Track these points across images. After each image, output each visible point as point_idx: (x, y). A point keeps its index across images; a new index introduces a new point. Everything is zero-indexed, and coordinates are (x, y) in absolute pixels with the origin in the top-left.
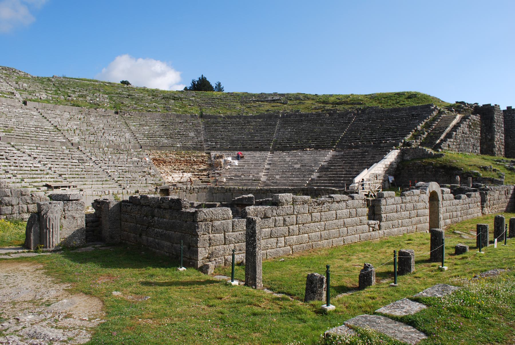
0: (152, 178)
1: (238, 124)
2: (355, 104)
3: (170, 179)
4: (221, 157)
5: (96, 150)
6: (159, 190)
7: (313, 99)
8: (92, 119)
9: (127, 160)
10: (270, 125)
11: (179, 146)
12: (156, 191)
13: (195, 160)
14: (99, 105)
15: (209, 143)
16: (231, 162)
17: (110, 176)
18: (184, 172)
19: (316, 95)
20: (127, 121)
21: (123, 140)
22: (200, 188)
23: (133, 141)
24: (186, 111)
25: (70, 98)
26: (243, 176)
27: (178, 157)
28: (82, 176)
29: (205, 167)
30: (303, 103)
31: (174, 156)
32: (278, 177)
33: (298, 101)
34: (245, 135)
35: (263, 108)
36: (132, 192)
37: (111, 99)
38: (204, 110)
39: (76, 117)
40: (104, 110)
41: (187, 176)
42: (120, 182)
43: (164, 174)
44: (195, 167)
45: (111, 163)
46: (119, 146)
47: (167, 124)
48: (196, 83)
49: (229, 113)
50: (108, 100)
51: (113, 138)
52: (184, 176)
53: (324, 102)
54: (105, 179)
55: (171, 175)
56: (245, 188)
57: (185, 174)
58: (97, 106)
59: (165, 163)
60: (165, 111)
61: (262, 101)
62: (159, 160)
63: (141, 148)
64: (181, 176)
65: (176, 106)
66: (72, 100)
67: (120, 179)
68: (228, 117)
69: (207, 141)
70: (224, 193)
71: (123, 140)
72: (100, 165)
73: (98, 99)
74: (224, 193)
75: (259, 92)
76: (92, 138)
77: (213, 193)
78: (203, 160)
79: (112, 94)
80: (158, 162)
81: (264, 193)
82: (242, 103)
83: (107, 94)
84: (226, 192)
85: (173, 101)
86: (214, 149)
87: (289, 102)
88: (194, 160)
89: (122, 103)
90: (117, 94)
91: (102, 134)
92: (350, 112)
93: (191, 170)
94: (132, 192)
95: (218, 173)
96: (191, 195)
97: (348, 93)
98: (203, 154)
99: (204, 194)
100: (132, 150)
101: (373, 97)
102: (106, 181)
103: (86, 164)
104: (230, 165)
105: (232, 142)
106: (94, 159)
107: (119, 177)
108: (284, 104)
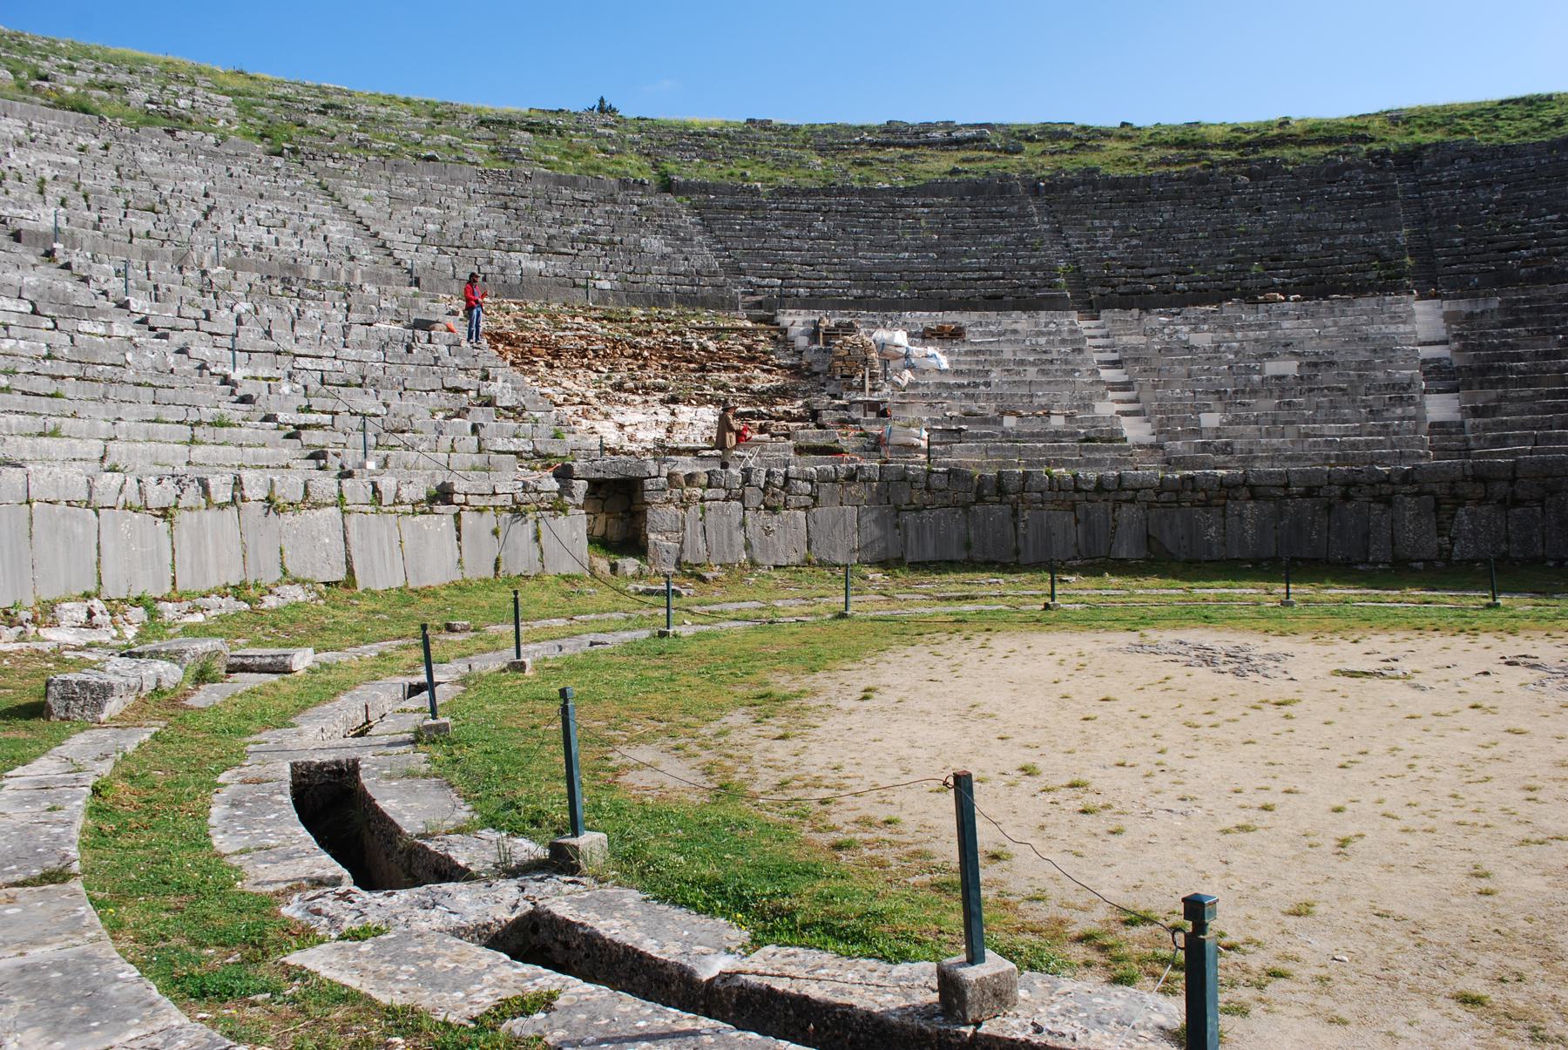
0: (512, 423)
2: (1339, 141)
4: (850, 328)
5: (164, 273)
6: (580, 487)
7: (1123, 138)
8: (145, 158)
9: (346, 331)
10: (1002, 215)
11: (606, 285)
12: (566, 490)
13: (712, 346)
14: (190, 121)
16: (907, 356)
17: (245, 399)
18: (674, 400)
19: (1123, 124)
20: (329, 181)
21: (314, 247)
22: (824, 478)
23: (365, 253)
24: (598, 169)
25: (46, 84)
26: (1010, 422)
27: (620, 332)
29: (777, 380)
30: (1098, 148)
31: (596, 326)
32: (1210, 420)
33: (1067, 145)
35: (925, 167)
36: (407, 493)
37: (246, 110)
38: (671, 167)
39: (62, 139)
40: (211, 138)
41: (698, 421)
42: (315, 438)
43: (568, 410)
44: (724, 377)
46: (294, 266)
47: (522, 203)
49: (784, 179)
50: (232, 112)
52: (682, 418)
53: (1181, 144)
54: (207, 414)
55: (607, 416)
56: (1092, 475)
57: (685, 413)
58: (175, 123)
59: (557, 355)
60: (502, 164)
61: (908, 146)
62: (524, 339)
63: (417, 283)
65: (546, 150)
66: (59, 92)
67: (312, 418)
68: (789, 192)
69: (741, 272)
70: (966, 507)
71: (314, 247)
72: (177, 339)
73: (182, 103)
74: (966, 507)
76: (142, 223)
77: (898, 510)
78: (749, 348)
81: (1206, 504)
82: (821, 151)
83: (226, 94)
84: (980, 499)
85: (527, 135)
86: (786, 300)
87: (1027, 146)
88: (705, 349)
89: (302, 125)
90: (271, 97)
91: (198, 216)
92: (1347, 166)
94: (407, 493)
95: (872, 406)
96: (773, 522)
97: (1275, 115)
98: (740, 324)
99: (851, 511)
100: (371, 289)
101: (1395, 119)
102: (219, 423)
104: (911, 367)
105: (862, 276)
106: (139, 303)
107: (309, 409)
108: (1007, 151)
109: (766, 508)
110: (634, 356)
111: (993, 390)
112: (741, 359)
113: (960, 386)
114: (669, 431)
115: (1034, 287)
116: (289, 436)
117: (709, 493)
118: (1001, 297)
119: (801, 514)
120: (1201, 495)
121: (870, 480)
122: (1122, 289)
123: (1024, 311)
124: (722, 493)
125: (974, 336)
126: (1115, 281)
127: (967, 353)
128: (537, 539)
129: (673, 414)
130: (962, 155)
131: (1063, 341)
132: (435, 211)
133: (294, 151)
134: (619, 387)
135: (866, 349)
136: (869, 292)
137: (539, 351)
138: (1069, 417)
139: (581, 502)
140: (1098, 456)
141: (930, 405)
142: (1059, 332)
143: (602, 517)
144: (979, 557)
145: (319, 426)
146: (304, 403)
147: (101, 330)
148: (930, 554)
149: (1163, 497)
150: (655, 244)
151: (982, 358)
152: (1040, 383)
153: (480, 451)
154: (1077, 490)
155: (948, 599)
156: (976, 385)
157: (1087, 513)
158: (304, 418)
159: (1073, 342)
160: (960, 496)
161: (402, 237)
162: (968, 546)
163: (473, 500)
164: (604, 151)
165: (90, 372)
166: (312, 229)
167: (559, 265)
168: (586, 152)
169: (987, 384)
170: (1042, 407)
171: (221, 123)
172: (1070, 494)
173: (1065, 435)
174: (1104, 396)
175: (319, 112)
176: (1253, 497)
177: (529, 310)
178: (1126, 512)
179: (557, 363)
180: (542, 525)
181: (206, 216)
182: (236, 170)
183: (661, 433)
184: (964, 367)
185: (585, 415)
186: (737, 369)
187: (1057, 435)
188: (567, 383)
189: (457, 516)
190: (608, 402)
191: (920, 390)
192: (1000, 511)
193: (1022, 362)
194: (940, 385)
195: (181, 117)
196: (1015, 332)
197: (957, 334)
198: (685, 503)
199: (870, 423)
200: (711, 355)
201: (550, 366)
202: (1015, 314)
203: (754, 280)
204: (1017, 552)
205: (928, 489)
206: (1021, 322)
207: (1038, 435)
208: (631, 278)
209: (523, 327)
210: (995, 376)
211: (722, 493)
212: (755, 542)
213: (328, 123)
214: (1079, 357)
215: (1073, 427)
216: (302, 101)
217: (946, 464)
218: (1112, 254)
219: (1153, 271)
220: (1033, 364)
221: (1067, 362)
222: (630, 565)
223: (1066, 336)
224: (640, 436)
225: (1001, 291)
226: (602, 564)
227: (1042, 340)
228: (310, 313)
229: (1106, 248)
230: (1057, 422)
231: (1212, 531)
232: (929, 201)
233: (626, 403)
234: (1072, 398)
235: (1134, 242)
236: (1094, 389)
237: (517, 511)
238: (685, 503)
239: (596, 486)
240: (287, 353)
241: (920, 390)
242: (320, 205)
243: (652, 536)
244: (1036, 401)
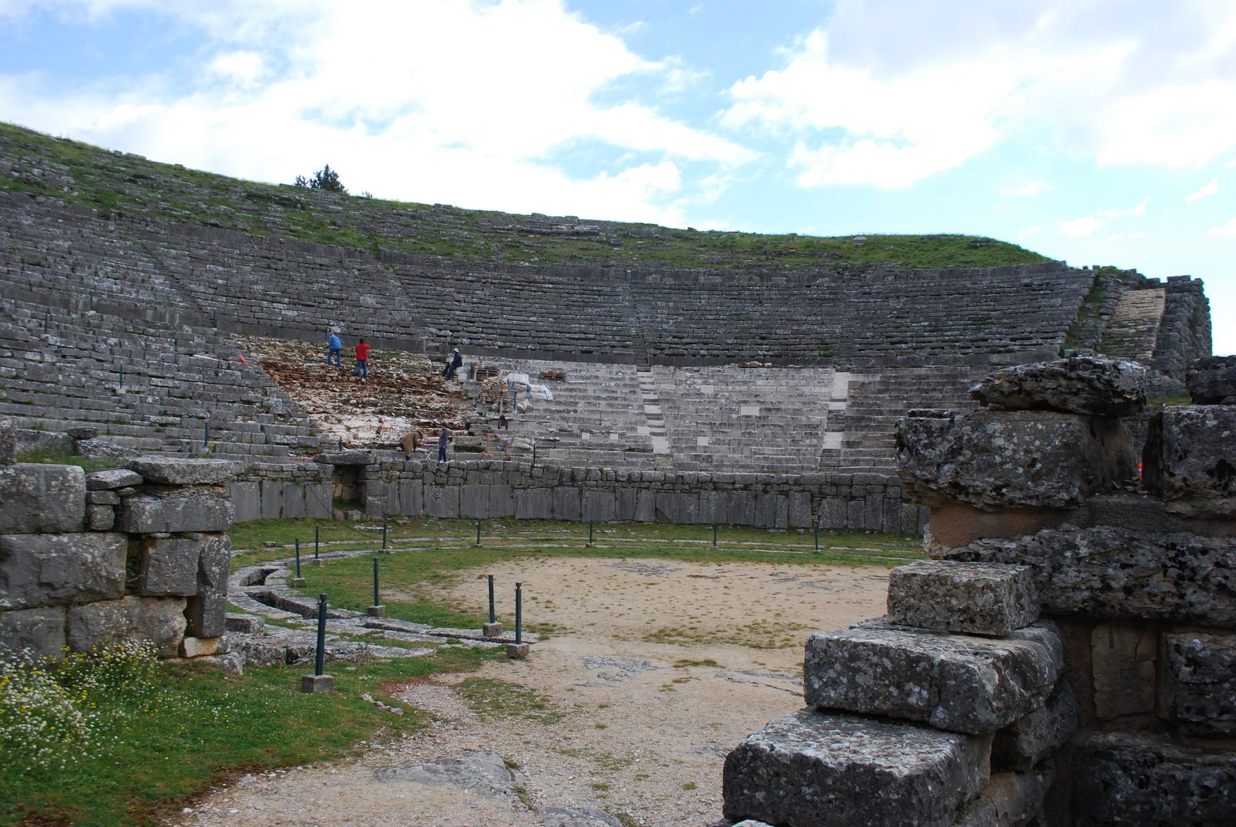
1: (504, 284)
3: (340, 433)
8: (27, 221)
10: (600, 293)
13: (405, 375)
14: (45, 188)
15: (434, 330)
16: (528, 390)
18: (381, 412)
21: (145, 296)
24: (330, 239)
26: (586, 436)
28: (23, 397)
32: (703, 441)
34: (534, 314)
37: (78, 176)
41: (397, 427)
43: (315, 417)
44: (413, 398)
45: (122, 361)
48: (309, 185)
51: (108, 284)
55: (340, 421)
57: (388, 421)
59: (307, 380)
64: (376, 424)
69: (425, 324)
70: (552, 488)
72: (81, 363)
73: (36, 171)
74: (552, 488)
75: (525, 210)
76: (35, 275)
77: (513, 488)
78: (429, 379)
79: (82, 165)
80: (289, 375)
81: (689, 492)
83: (64, 163)
84: (561, 484)
88: (401, 378)
90: (96, 167)
93: (403, 406)
103: (29, 355)
104: (530, 398)
105: (505, 333)
107: (165, 414)
110: (357, 382)
111: (578, 415)
112: (424, 387)
113: (558, 412)
114: (378, 432)
115: (613, 347)
116: (158, 431)
119: (456, 488)
120: (687, 487)
122: (667, 351)
123: (604, 363)
124: (411, 475)
125: (572, 379)
126: (664, 346)
127: (566, 390)
128: (304, 497)
129: (380, 421)
130: (581, 245)
131: (625, 385)
132: (221, 269)
133: (120, 215)
134: (346, 402)
135: (501, 385)
137: (296, 375)
138: (622, 436)
140: (634, 460)
141: (540, 423)
142: (623, 379)
143: (340, 486)
144: (559, 517)
145: (173, 424)
146: (162, 409)
147: (38, 358)
148: (530, 515)
149: (666, 486)
150: (369, 300)
151: (574, 394)
152: (607, 413)
153: (267, 442)
154: (617, 481)
155: (537, 540)
156: (569, 412)
157: (622, 495)
158: (165, 419)
159: (632, 386)
160: (550, 482)
161: (202, 289)
162: (553, 511)
163: (270, 475)
164: (334, 224)
165: (42, 387)
166: (143, 281)
167: (307, 314)
168: (322, 224)
169: (575, 411)
170: (606, 427)
171: (66, 189)
172: (612, 483)
173: (617, 446)
174: (644, 423)
175: (130, 181)
176: (715, 489)
177: (288, 346)
178: (644, 495)
179: (307, 385)
180: (308, 489)
181: (73, 270)
182: (86, 232)
183: (373, 434)
184: (562, 399)
185: (326, 419)
186: (421, 393)
187: (612, 447)
188: (316, 399)
189: (261, 483)
190: (340, 412)
191: (534, 413)
192: (573, 491)
193: (598, 398)
194: (546, 410)
195: (38, 184)
196: (597, 377)
197: (560, 377)
198: (389, 479)
199: (501, 433)
200: (405, 383)
201: (304, 387)
202: (598, 365)
204: (581, 516)
205: (531, 477)
206: (601, 370)
207: (601, 445)
208: (355, 325)
209: (286, 359)
210: (581, 406)
211: (411, 475)
212: (428, 504)
213: (138, 191)
214: (633, 397)
215: (623, 442)
216: (118, 171)
217: (545, 461)
218: (665, 326)
219: (688, 340)
220: (605, 399)
221: (625, 399)
222: (356, 515)
223: (628, 382)
224: (361, 435)
226: (340, 514)
227: (612, 384)
228: (153, 347)
229: (662, 322)
230: (614, 438)
231: (692, 507)
232: (554, 279)
233: (351, 413)
234: (625, 423)
235: (681, 318)
236: (639, 418)
237: (294, 480)
238: (389, 479)
239: (338, 467)
240: (145, 375)
241: (534, 413)
242: (145, 263)
243: (370, 498)
244: (603, 424)
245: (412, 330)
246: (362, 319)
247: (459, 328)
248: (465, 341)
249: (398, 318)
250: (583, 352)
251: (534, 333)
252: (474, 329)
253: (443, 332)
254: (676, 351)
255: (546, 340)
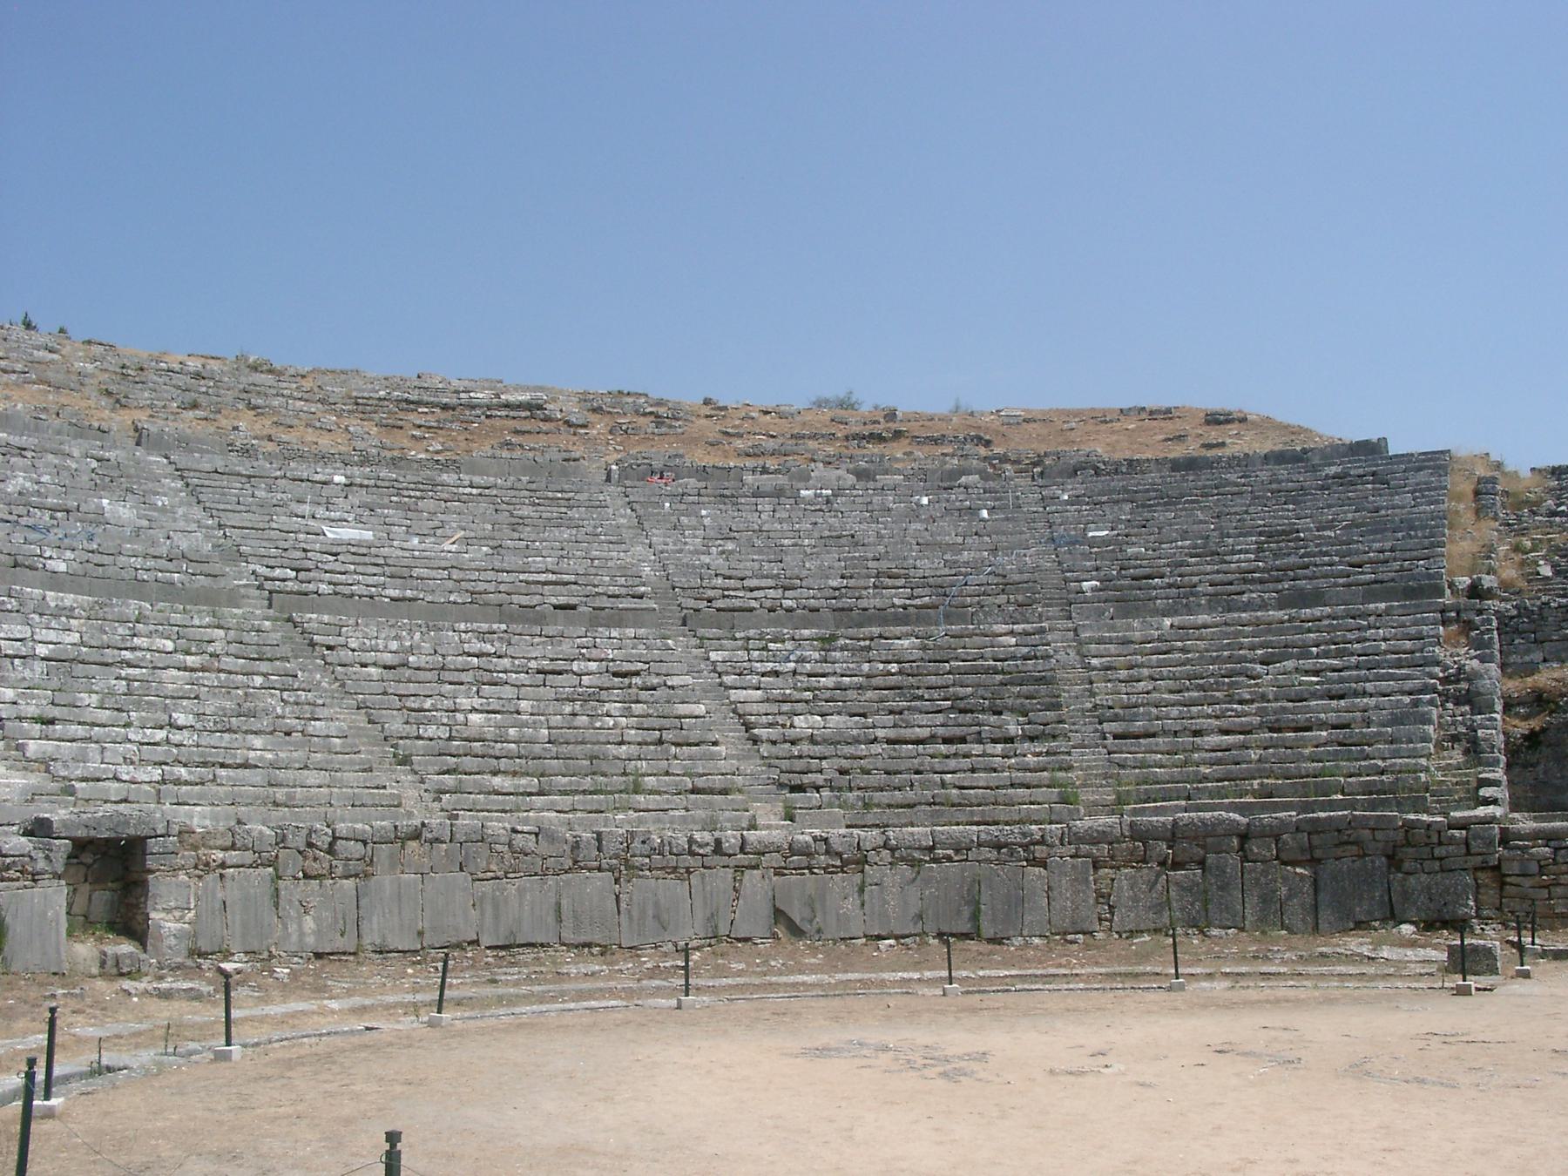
109: (306, 876)
117: (233, 856)
118: (573, 607)
119: (349, 884)
121: (437, 840)
122: (720, 604)
124: (249, 857)
126: (710, 593)
136: (409, 593)
139: (60, 870)
203: (261, 570)
208: (97, 558)
225: (573, 601)
232: (477, 479)
239: (81, 846)
245: (216, 568)
246: (110, 545)
247: (309, 564)
248: (324, 588)
249: (184, 545)
250: (556, 607)
251: (456, 574)
252: (338, 567)
253: (278, 572)
254: (737, 603)
255: (481, 586)
